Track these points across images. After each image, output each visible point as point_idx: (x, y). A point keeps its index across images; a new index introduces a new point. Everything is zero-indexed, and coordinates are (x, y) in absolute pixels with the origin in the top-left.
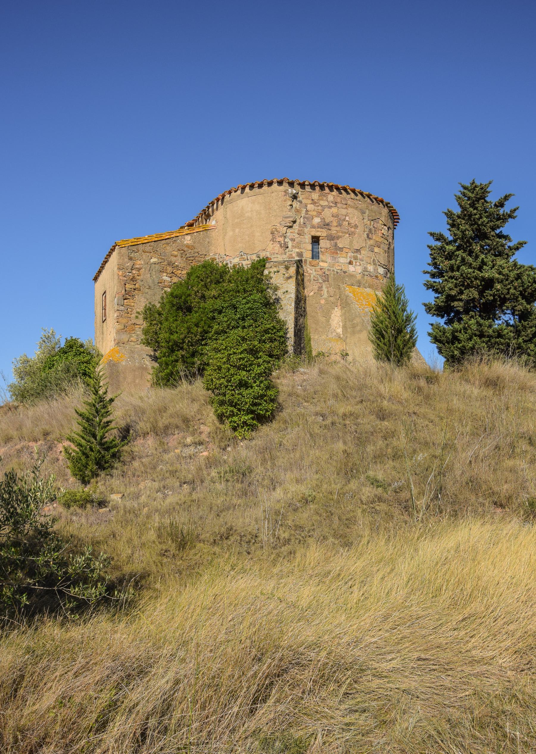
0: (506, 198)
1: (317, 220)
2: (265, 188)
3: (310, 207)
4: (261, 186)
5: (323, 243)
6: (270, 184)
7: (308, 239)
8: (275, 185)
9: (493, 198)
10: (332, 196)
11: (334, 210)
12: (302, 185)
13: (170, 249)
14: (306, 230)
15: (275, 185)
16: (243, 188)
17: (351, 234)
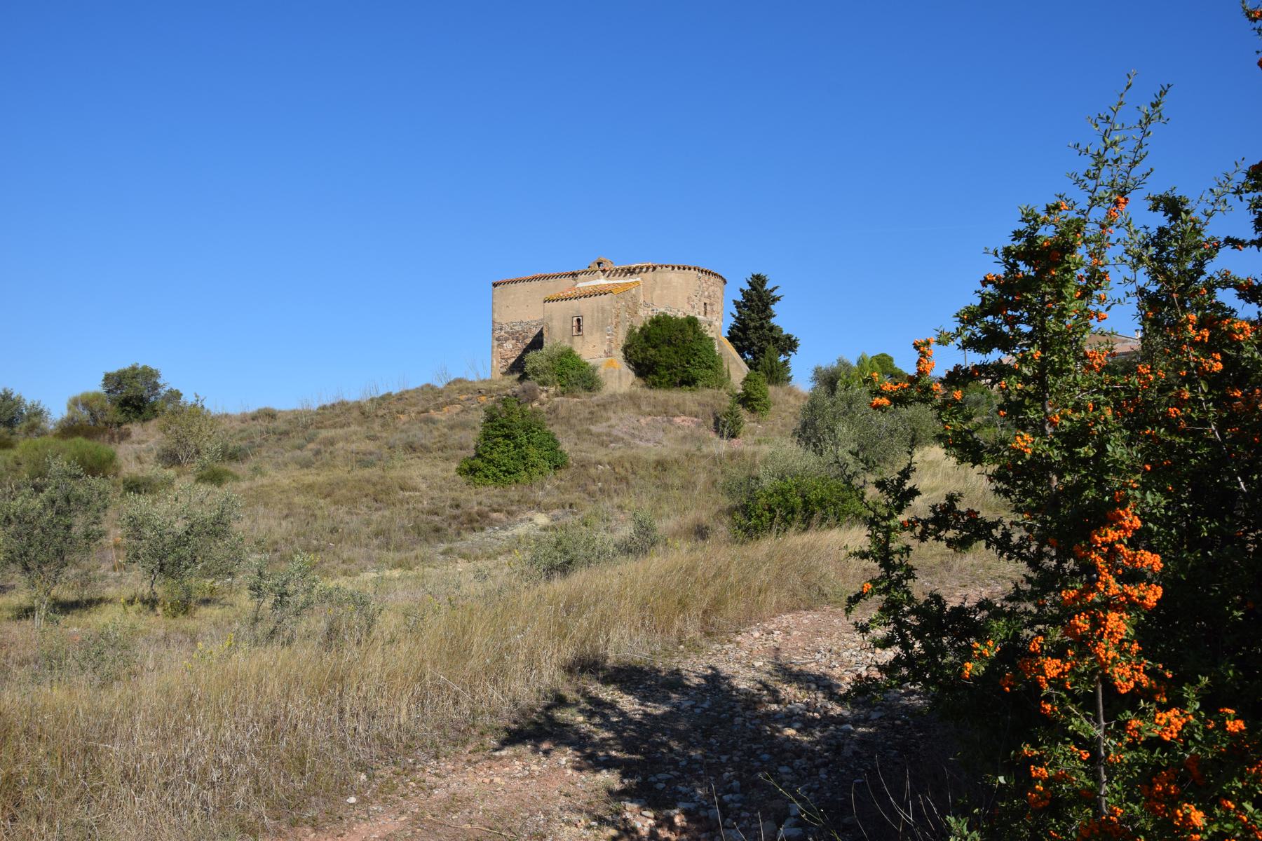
0: (776, 288)
1: (706, 293)
2: (687, 270)
3: (704, 285)
4: (684, 269)
5: (708, 307)
6: (690, 269)
7: (703, 305)
8: (692, 270)
9: (768, 286)
10: (713, 278)
11: (713, 288)
12: (702, 271)
13: (628, 297)
14: (703, 299)
15: (692, 270)
16: (673, 268)
17: (717, 302)
